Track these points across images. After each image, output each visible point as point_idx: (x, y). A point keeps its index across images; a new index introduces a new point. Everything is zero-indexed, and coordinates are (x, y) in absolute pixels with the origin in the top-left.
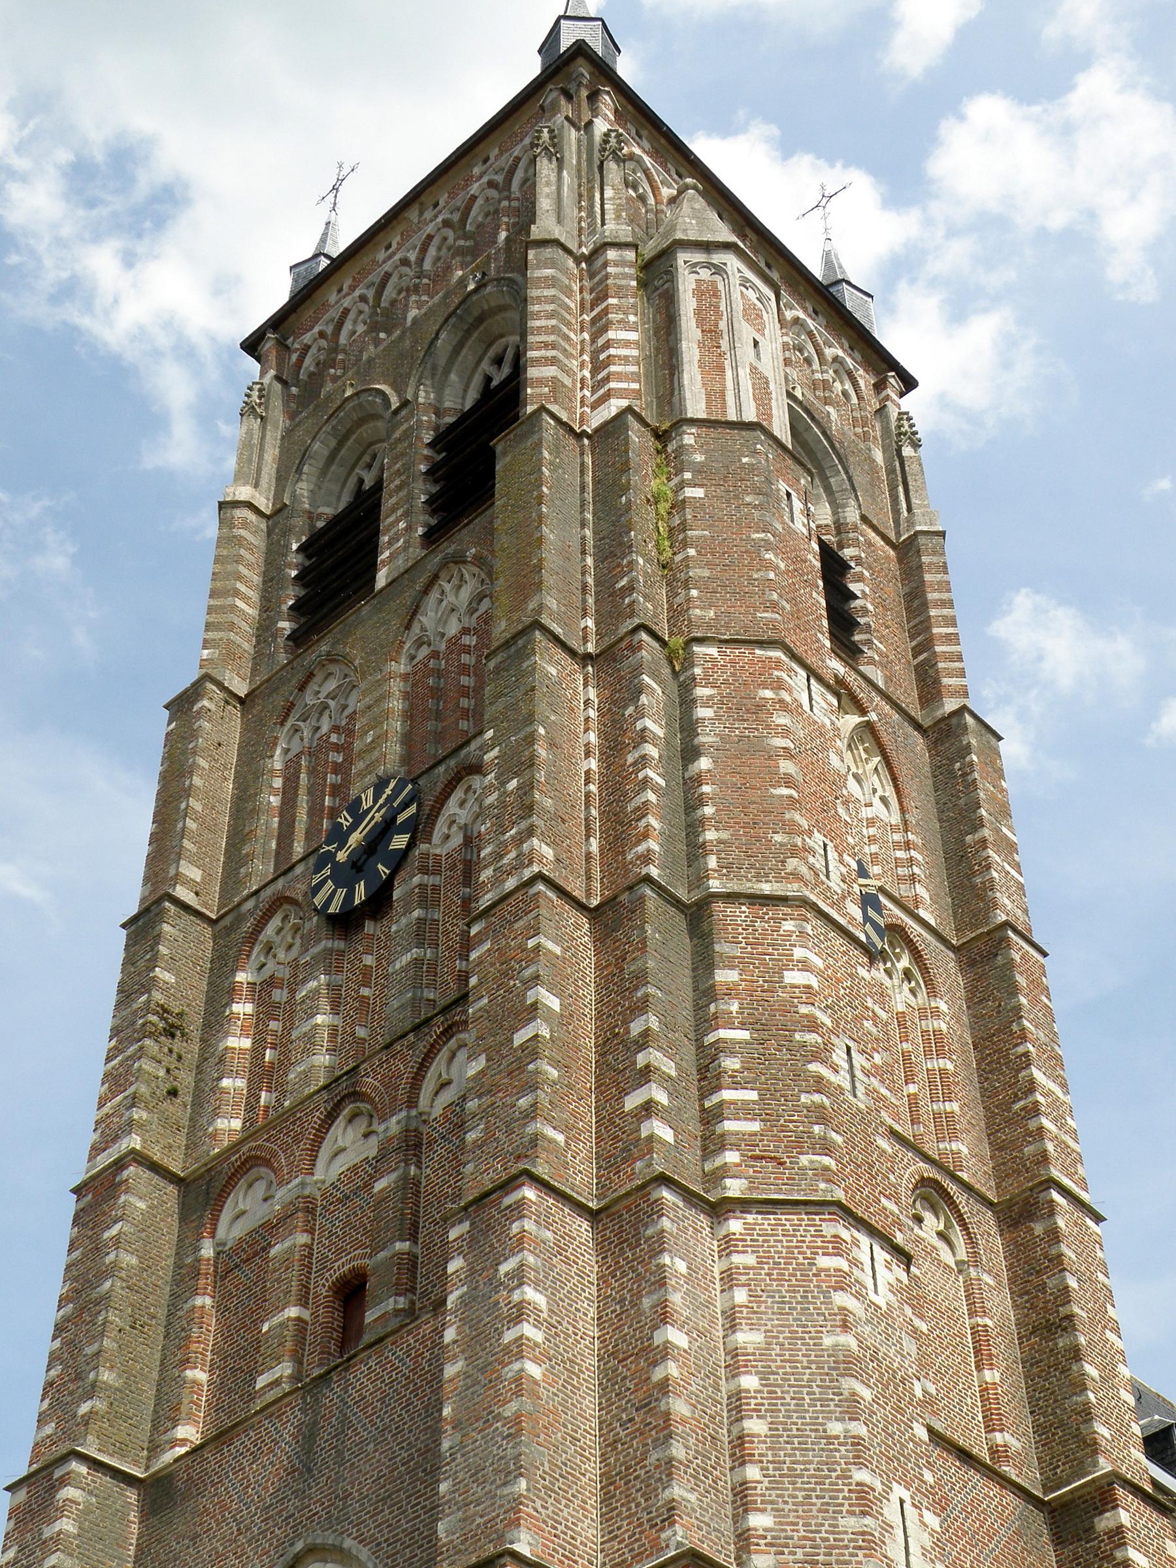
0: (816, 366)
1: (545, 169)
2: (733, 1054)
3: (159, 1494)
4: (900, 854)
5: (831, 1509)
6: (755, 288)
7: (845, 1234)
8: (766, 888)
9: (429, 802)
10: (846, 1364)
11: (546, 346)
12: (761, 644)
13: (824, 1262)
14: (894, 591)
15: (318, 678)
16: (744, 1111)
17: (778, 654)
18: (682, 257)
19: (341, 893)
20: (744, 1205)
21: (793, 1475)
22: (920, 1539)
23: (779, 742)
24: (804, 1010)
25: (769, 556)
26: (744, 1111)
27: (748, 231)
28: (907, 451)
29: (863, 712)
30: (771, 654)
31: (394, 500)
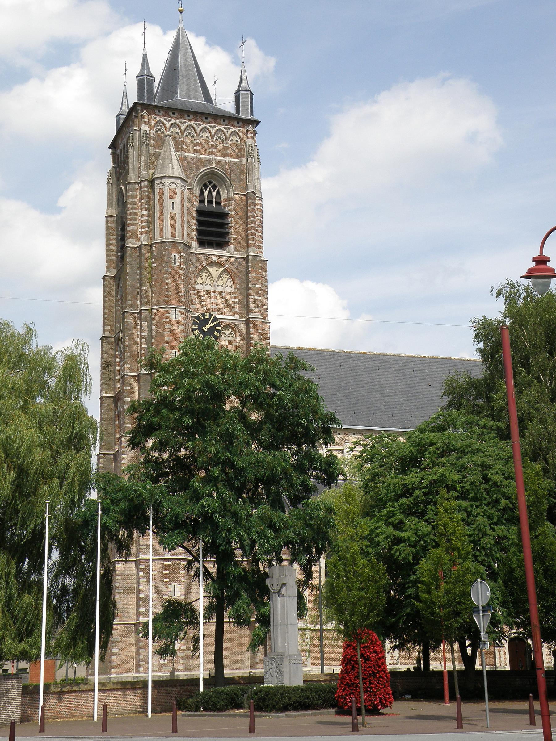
0: (225, 142)
1: (131, 150)
4: (233, 300)
6: (173, 183)
11: (131, 219)
17: (168, 309)
18: (156, 182)
23: (166, 333)
25: (167, 281)
27: (198, 115)
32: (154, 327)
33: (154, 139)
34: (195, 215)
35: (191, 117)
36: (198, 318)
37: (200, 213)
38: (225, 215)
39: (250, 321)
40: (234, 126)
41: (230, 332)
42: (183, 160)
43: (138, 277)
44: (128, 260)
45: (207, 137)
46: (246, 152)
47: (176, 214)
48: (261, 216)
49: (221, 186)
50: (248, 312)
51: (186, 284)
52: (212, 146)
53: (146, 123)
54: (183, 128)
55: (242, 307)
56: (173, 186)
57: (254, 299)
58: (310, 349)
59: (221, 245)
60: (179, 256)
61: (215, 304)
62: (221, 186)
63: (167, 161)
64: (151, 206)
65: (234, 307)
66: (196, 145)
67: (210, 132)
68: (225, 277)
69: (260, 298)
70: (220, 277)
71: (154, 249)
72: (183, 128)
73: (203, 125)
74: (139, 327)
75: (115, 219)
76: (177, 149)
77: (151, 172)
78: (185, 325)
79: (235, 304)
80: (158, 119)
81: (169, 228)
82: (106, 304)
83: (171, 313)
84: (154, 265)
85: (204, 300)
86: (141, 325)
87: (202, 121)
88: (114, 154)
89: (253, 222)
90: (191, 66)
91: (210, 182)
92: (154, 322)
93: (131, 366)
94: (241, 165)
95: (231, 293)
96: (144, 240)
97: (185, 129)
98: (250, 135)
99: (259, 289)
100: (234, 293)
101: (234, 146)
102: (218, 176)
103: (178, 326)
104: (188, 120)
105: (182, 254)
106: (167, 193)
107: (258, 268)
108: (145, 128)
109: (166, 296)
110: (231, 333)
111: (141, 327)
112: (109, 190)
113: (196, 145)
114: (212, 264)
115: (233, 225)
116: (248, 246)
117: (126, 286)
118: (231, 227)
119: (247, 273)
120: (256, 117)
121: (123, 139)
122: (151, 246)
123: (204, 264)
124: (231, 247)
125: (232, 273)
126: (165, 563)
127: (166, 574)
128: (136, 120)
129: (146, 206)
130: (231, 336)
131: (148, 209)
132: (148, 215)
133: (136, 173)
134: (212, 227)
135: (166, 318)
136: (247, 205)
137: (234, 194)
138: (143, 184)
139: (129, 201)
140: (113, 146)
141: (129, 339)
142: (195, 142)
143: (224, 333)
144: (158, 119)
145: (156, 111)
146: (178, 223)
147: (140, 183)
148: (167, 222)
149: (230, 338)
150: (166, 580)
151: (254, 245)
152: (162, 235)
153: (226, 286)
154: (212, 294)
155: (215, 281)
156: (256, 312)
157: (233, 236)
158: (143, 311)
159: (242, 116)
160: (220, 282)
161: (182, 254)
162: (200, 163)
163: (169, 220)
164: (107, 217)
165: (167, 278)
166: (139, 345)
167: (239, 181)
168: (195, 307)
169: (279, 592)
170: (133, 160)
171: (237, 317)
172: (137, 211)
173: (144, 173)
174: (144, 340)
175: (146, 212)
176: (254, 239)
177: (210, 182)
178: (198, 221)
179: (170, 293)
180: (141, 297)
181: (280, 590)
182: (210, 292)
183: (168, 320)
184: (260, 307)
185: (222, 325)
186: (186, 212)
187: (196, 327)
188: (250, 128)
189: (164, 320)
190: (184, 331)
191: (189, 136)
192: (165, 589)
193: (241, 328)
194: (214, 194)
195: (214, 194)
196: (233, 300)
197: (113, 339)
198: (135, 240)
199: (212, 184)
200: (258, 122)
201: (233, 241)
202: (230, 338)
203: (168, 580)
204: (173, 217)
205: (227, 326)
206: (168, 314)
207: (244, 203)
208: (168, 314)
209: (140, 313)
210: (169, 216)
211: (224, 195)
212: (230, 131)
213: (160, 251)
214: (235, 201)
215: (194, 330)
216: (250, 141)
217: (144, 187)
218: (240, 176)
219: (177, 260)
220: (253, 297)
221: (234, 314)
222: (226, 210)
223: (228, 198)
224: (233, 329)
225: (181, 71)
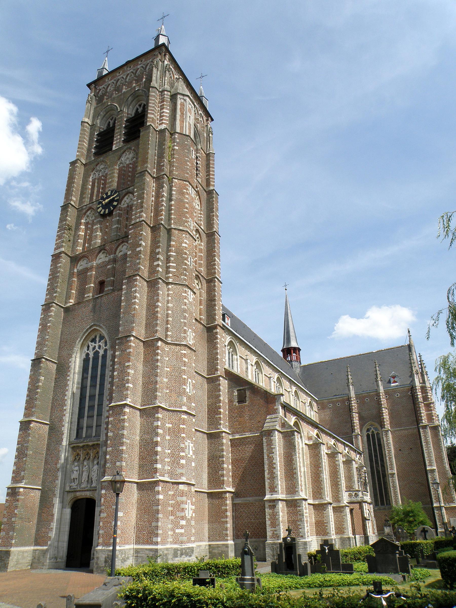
1: (155, 70)
2: (172, 257)
3: (67, 310)
4: (199, 215)
5: (180, 333)
6: (191, 105)
7: (187, 290)
8: (181, 228)
9: (121, 197)
10: (185, 311)
11: (152, 110)
12: (185, 181)
13: (183, 294)
14: (205, 163)
15: (100, 164)
16: (173, 267)
17: (188, 183)
18: (179, 96)
19: (103, 210)
20: (172, 283)
21: (175, 327)
22: (192, 337)
23: (186, 200)
24: (185, 251)
25: (188, 163)
26: (173, 267)
27: (189, 87)
28: (211, 135)
31: (117, 131)
126: (183, 416)
127: (184, 429)
150: (183, 435)
192: (182, 445)
203: (184, 435)
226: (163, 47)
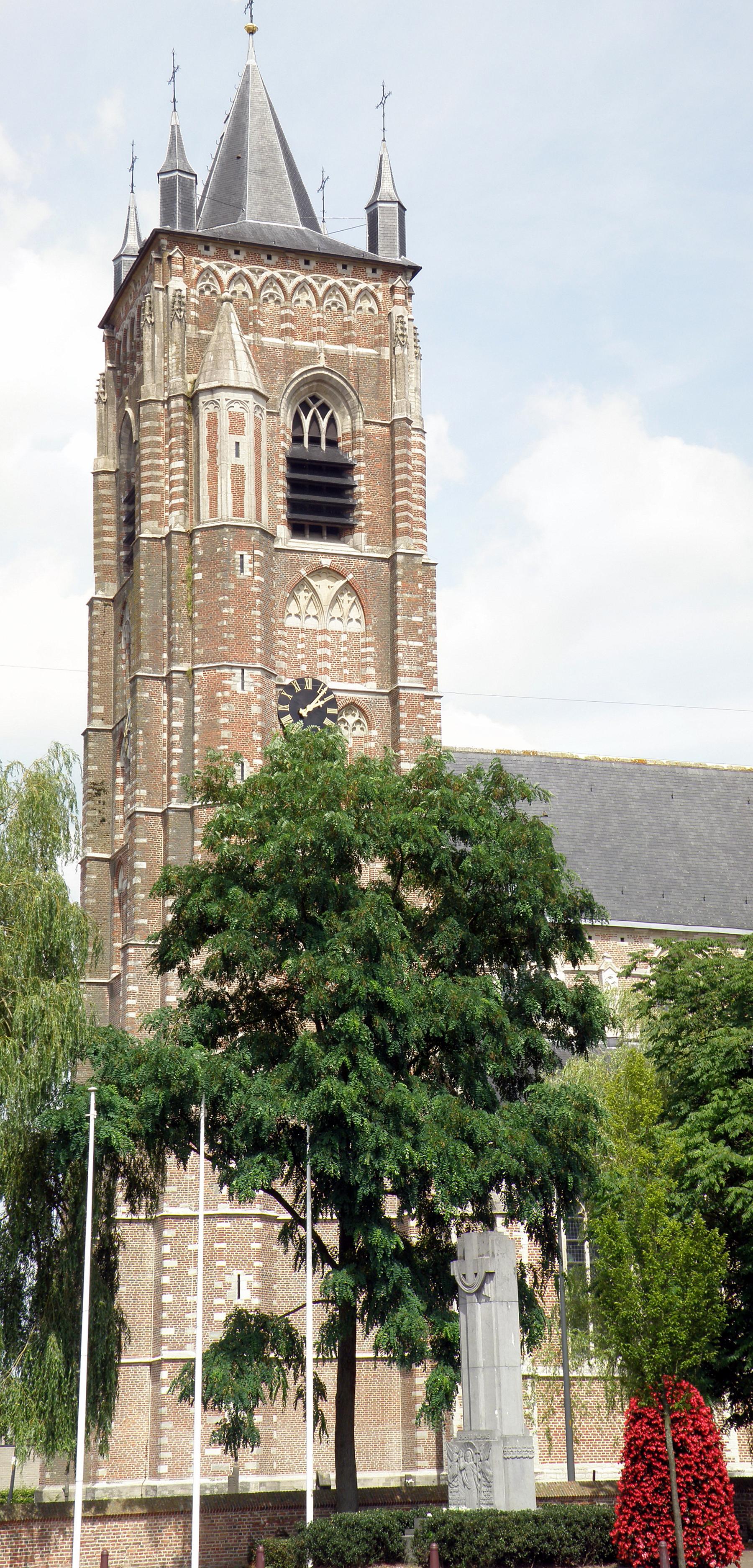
0: (345, 311)
1: (147, 332)
4: (363, 650)
6: (237, 401)
11: (149, 479)
14: (382, 464)
17: (227, 671)
18: (202, 399)
23: (223, 721)
25: (225, 611)
27: (289, 255)
29: (344, 578)
30: (222, 671)
32: (197, 710)
33: (197, 308)
34: (283, 469)
35: (275, 259)
36: (289, 688)
37: (294, 464)
38: (346, 469)
39: (398, 694)
40: (366, 279)
41: (357, 718)
42: (257, 352)
43: (165, 601)
44: (142, 566)
45: (308, 302)
46: (392, 334)
47: (243, 467)
48: (423, 470)
49: (338, 405)
50: (394, 675)
51: (266, 616)
52: (319, 322)
53: (179, 274)
54: (257, 284)
55: (382, 665)
56: (237, 408)
57: (409, 647)
58: (527, 754)
59: (337, 532)
60: (250, 557)
61: (325, 658)
62: (338, 405)
63: (225, 355)
64: (192, 450)
65: (366, 665)
66: (284, 319)
67: (315, 292)
68: (347, 599)
69: (421, 644)
70: (336, 600)
71: (197, 541)
72: (257, 284)
73: (301, 278)
74: (165, 708)
75: (114, 479)
76: (245, 328)
77: (190, 378)
78: (262, 704)
79: (369, 659)
80: (204, 264)
81: (230, 496)
82: (96, 660)
83: (233, 678)
84: (198, 576)
85: (303, 651)
86: (171, 706)
87: (298, 268)
88: (109, 340)
89: (406, 483)
90: (272, 148)
91: (315, 399)
92: (197, 698)
93: (149, 793)
94: (380, 361)
95: (357, 636)
96: (176, 522)
97: (262, 286)
98: (399, 296)
99: (417, 626)
100: (365, 634)
101: (364, 321)
102: (332, 386)
103: (248, 707)
104: (268, 266)
105: (257, 552)
106: (224, 423)
107: (416, 581)
108: (177, 283)
109: (224, 642)
110: (359, 722)
111: (170, 709)
112: (100, 416)
113: (284, 319)
114: (320, 572)
115: (363, 489)
116: (395, 534)
117: (139, 621)
118: (360, 493)
119: (393, 590)
120: (411, 258)
121: (129, 308)
122: (191, 535)
123: (303, 572)
124: (360, 537)
125: (362, 592)
128: (158, 267)
129: (181, 451)
130: (358, 727)
131: (186, 457)
132: (186, 471)
133: (160, 379)
134: (319, 495)
135: (224, 688)
136: (393, 447)
137: (366, 422)
138: (173, 404)
139: (144, 440)
140: (108, 322)
141: (146, 734)
142: (283, 312)
143: (344, 721)
144: (204, 264)
145: (201, 248)
146: (249, 487)
147: (168, 402)
148: (225, 484)
149: (358, 732)
151: (407, 532)
152: (214, 512)
153: (348, 620)
154: (320, 638)
155: (326, 609)
156: (411, 674)
157: (364, 513)
158: (174, 675)
159: (383, 255)
160: (336, 612)
161: (257, 552)
162: (292, 359)
163: (230, 481)
164: (96, 474)
165: (225, 604)
166: (165, 749)
167: (376, 395)
168: (283, 665)
169: (479, 1292)
170: (153, 353)
171: (372, 686)
172: (161, 462)
173: (175, 380)
174: (176, 738)
175: (181, 464)
176: (407, 519)
177: (315, 399)
178: (289, 481)
179: (232, 636)
180: (171, 644)
181: (482, 1287)
182: (315, 632)
183: (227, 694)
184: (421, 664)
185: (341, 704)
186: (264, 462)
187: (287, 708)
188: (399, 282)
189: (219, 694)
190: (262, 717)
191: (271, 301)
193: (381, 711)
194: (323, 423)
195: (323, 423)
196: (363, 650)
197: (110, 735)
198: (156, 523)
199: (319, 403)
200: (415, 270)
201: (363, 524)
202: (358, 732)
204: (238, 472)
205: (351, 706)
206: (227, 682)
207: (387, 442)
208: (227, 682)
209: (168, 679)
210: (229, 472)
211: (344, 425)
212: (356, 289)
213: (208, 545)
214: (369, 437)
215: (281, 714)
216: (398, 310)
217: (177, 410)
218: (378, 384)
219: (247, 566)
220: (404, 643)
221: (365, 679)
222: (350, 457)
223: (353, 432)
224: (362, 711)
225: (252, 161)
226: (161, 236)
